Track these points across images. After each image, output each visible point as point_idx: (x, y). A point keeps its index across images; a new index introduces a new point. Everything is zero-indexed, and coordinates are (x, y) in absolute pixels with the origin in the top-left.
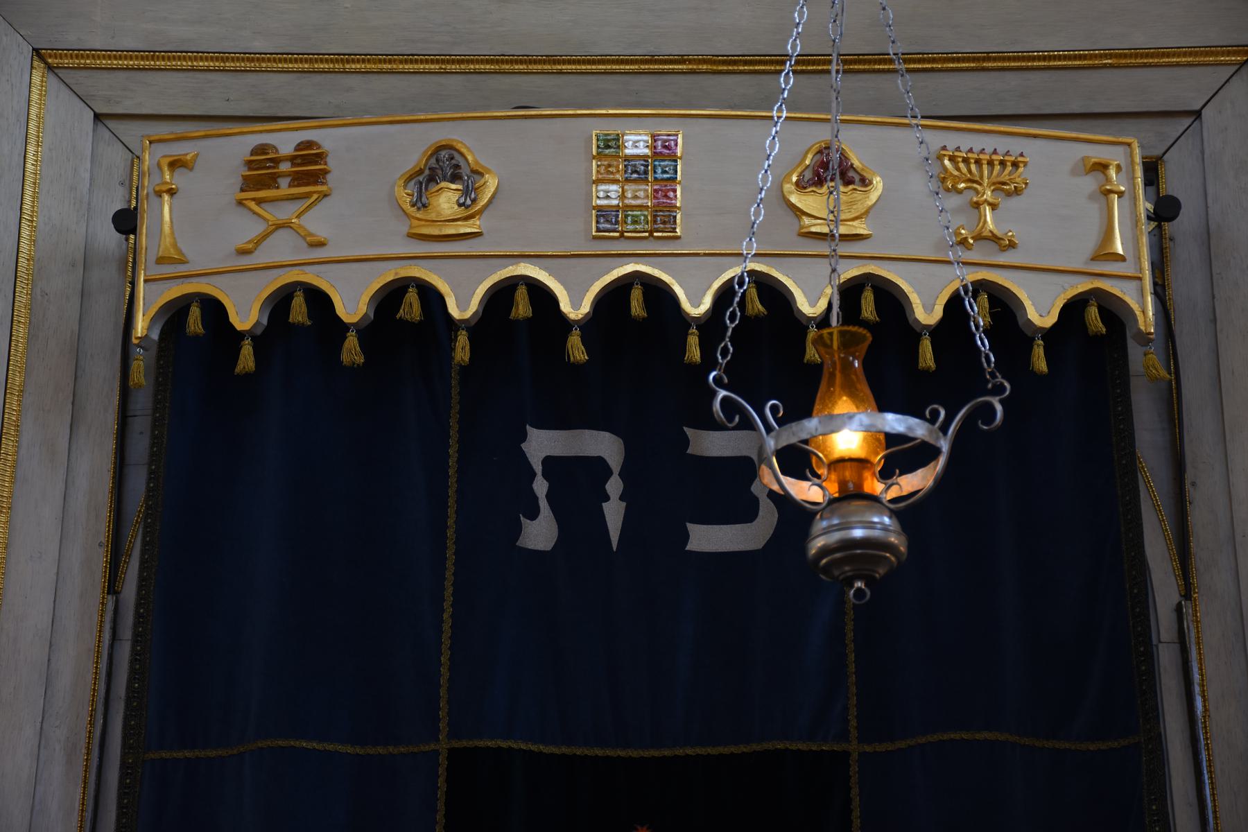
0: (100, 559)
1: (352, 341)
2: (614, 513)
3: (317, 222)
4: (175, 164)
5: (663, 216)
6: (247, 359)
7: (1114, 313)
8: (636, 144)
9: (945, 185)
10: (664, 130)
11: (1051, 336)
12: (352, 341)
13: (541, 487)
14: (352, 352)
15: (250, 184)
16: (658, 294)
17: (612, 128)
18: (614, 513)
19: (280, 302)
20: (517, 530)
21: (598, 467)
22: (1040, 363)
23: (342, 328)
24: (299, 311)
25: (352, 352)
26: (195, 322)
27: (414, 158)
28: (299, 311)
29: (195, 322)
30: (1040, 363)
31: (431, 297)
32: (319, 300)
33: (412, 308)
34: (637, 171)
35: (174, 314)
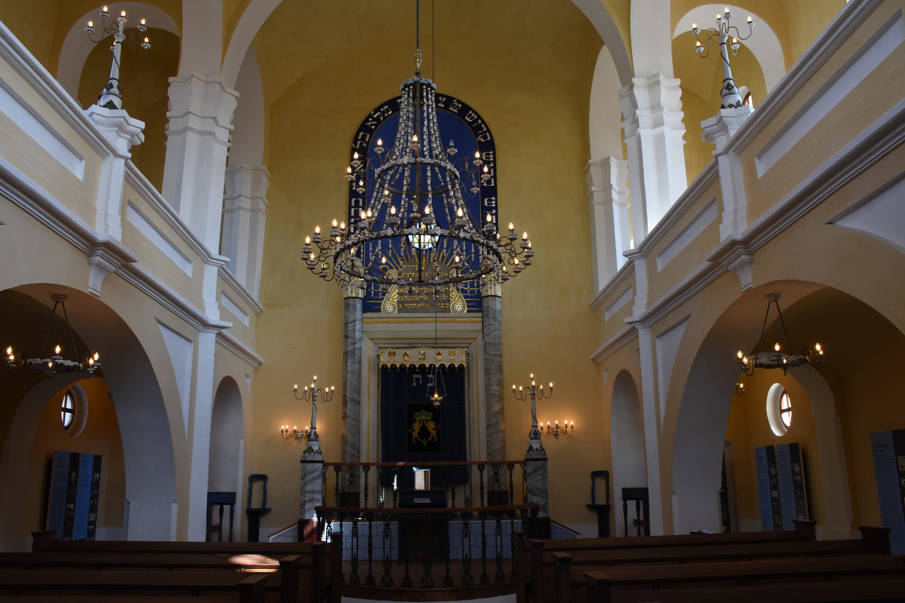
0: (377, 386)
1: (398, 369)
2: (421, 382)
3: (395, 358)
4: (382, 352)
5: (425, 359)
6: (389, 370)
7: (463, 365)
8: (422, 352)
9: (449, 354)
10: (425, 351)
11: (458, 368)
12: (398, 369)
13: (414, 380)
14: (398, 370)
15: (389, 355)
16: (424, 365)
17: (419, 351)
18: (421, 382)
19: (392, 365)
20: (412, 384)
21: (419, 378)
22: (456, 370)
23: (397, 368)
24: (394, 366)
25: (398, 370)
26: (385, 367)
27: (403, 353)
28: (394, 366)
29: (385, 367)
30: (456, 370)
31: (405, 365)
32: (395, 365)
33: (403, 366)
34: (423, 354)
35: (383, 366)
